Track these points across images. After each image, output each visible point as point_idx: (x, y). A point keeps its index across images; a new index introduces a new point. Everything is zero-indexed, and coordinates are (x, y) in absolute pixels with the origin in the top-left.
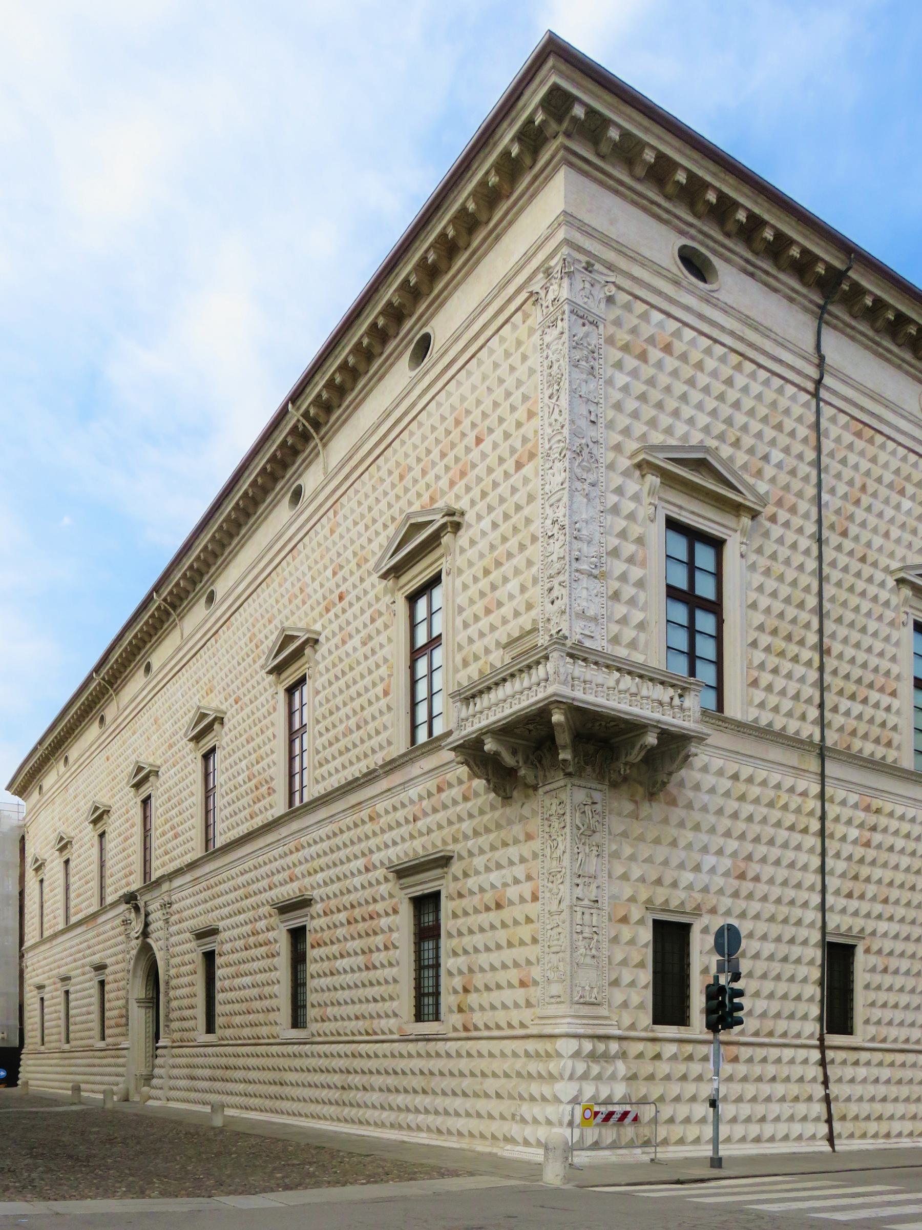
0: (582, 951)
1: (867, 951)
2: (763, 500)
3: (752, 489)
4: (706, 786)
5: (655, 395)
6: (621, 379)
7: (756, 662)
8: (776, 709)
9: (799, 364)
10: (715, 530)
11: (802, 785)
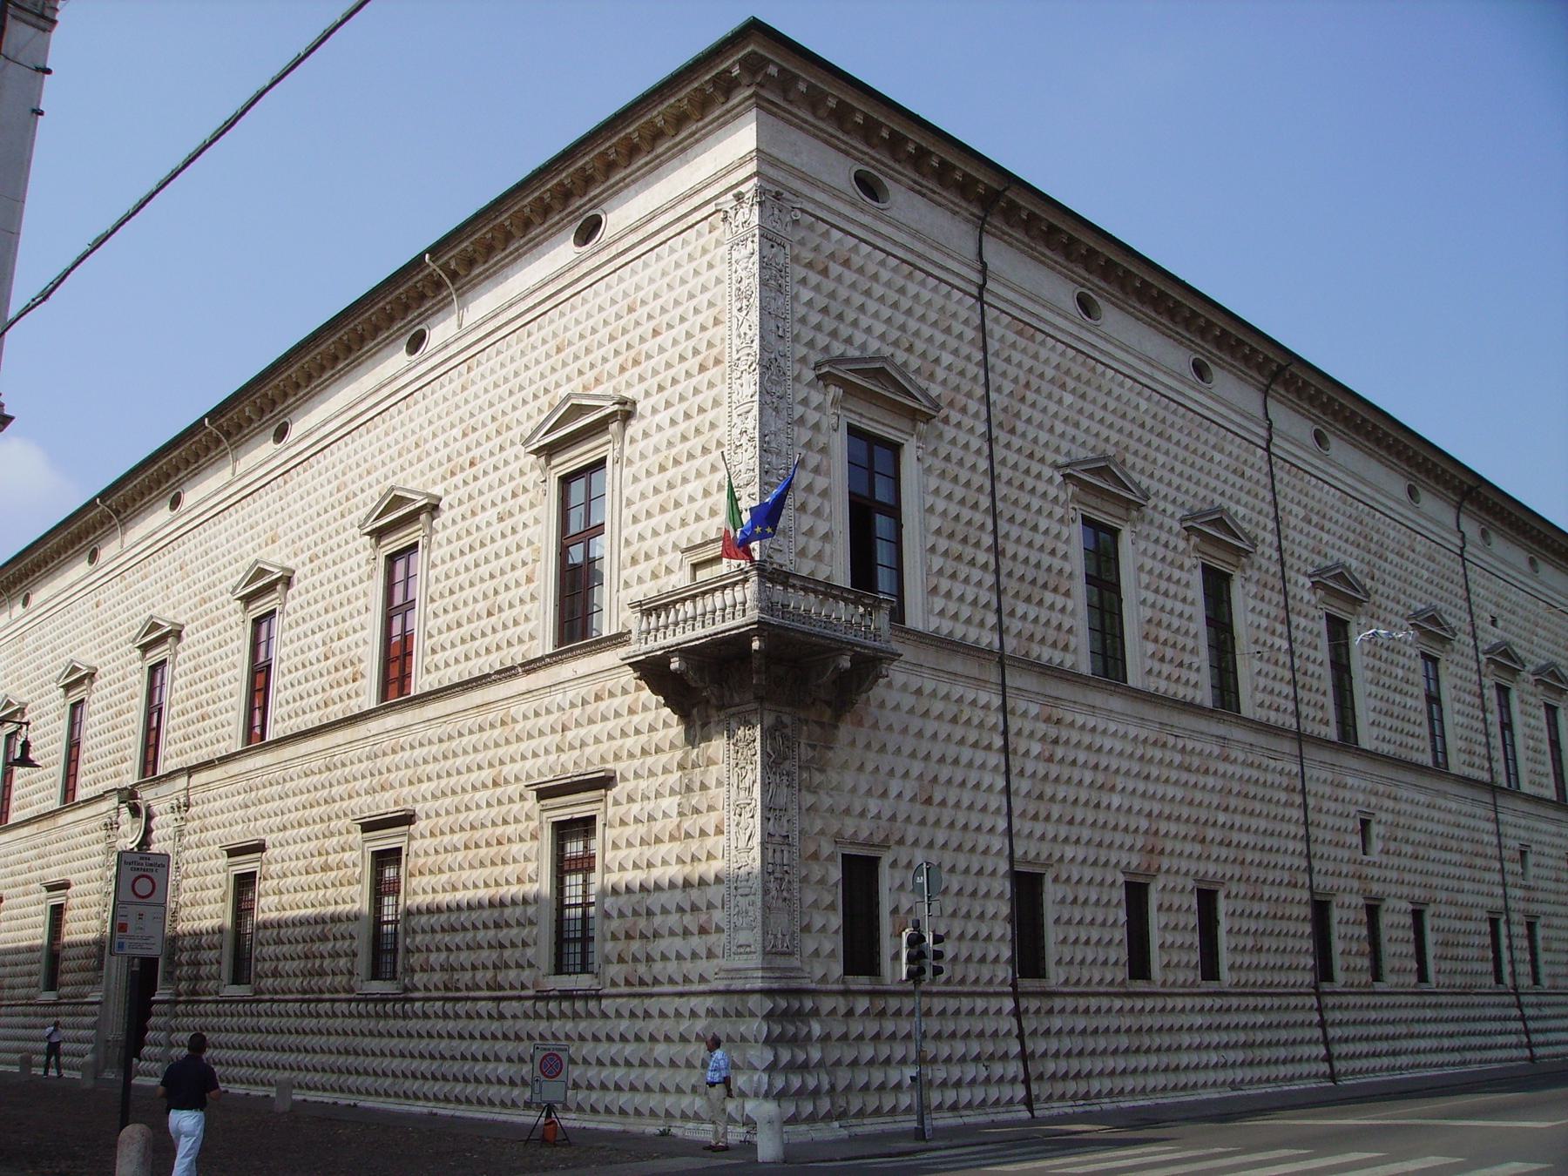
0: (774, 893)
1: (1056, 879)
2: (938, 408)
3: (925, 393)
4: (890, 704)
5: (836, 308)
6: (806, 295)
7: (935, 568)
8: (955, 617)
9: (964, 271)
10: (893, 435)
11: (983, 698)
